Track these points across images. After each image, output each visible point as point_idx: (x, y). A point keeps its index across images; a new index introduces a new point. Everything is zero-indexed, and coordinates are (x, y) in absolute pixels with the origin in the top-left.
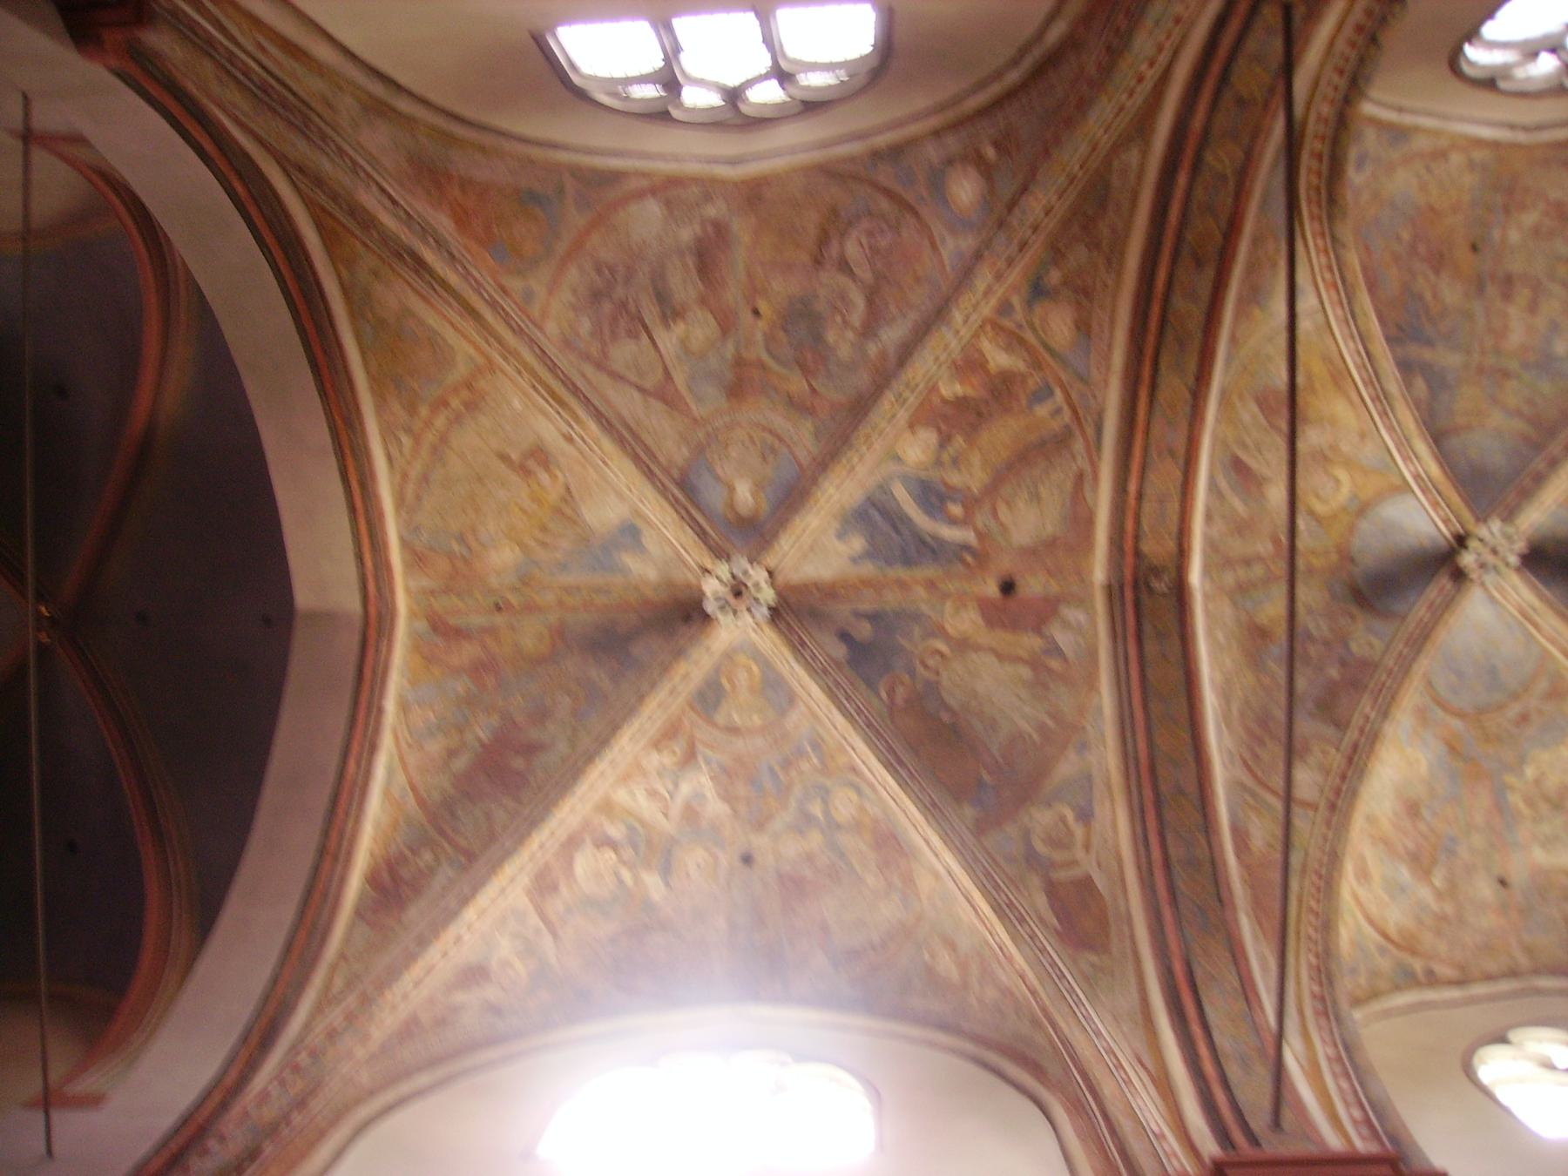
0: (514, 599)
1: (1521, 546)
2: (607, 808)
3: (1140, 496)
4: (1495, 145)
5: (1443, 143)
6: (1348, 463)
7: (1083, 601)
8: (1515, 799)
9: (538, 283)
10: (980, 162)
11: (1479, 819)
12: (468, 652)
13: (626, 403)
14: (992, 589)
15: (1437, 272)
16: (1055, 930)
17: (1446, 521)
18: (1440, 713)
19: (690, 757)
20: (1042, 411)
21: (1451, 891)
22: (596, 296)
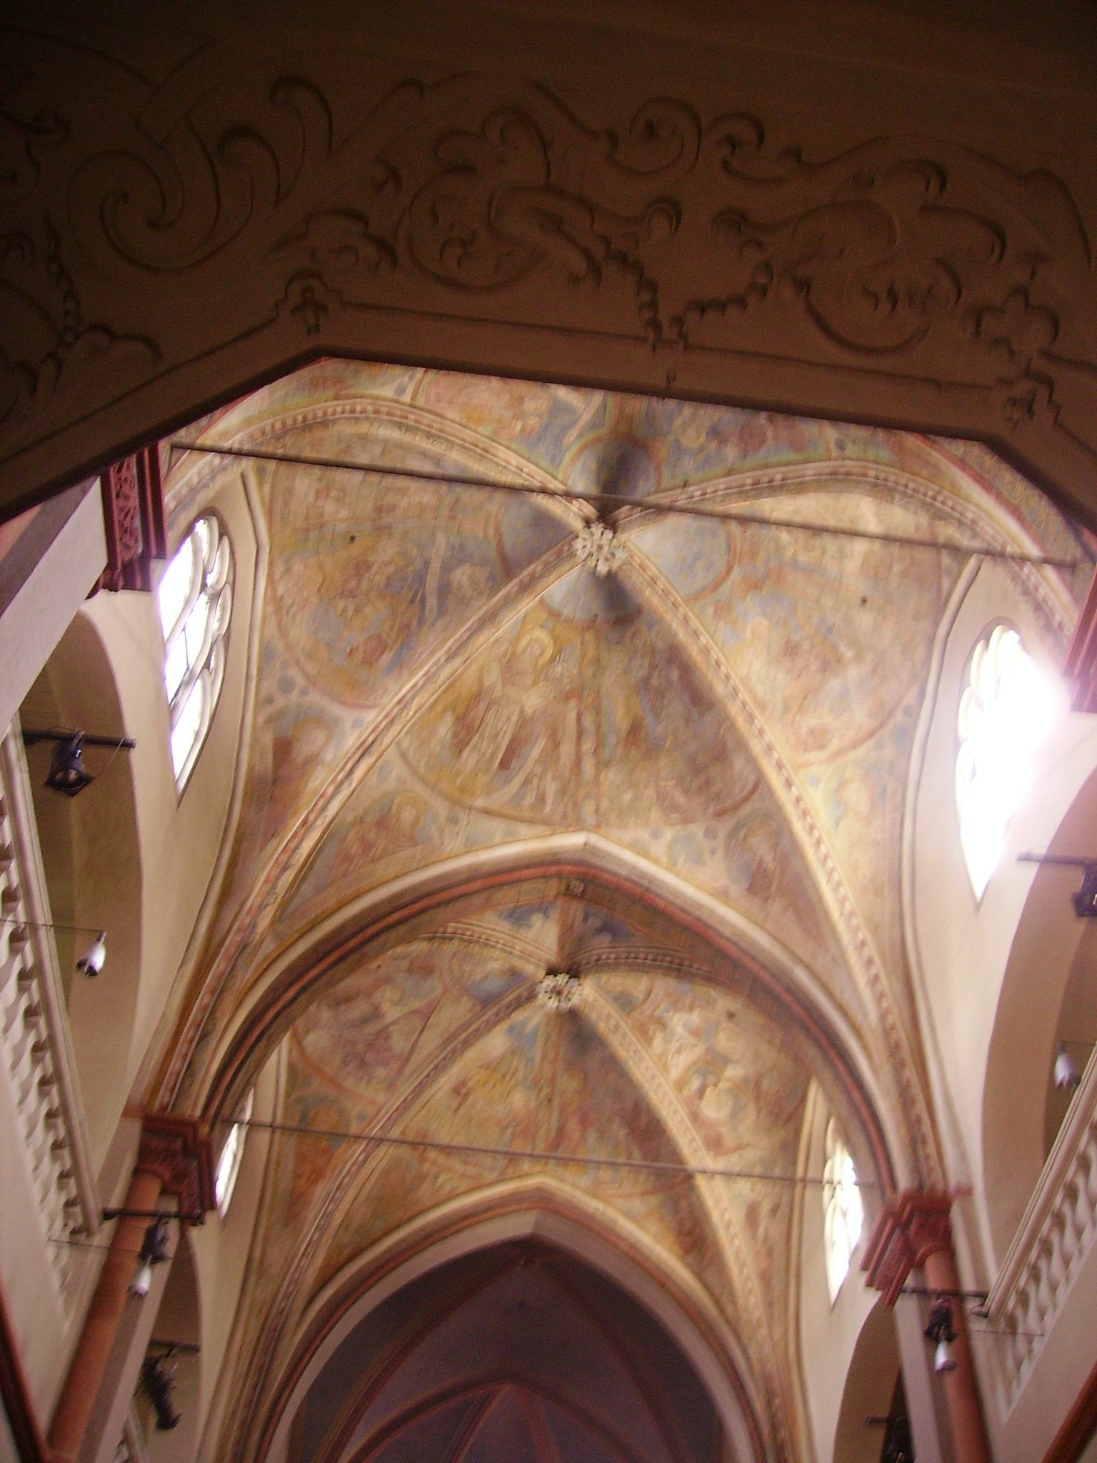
0: (546, 1091)
2: (680, 1085)
5: (271, 609)
9: (355, 1109)
12: (573, 1126)
13: (430, 1041)
18: (726, 587)
19: (662, 1024)
22: (363, 1065)
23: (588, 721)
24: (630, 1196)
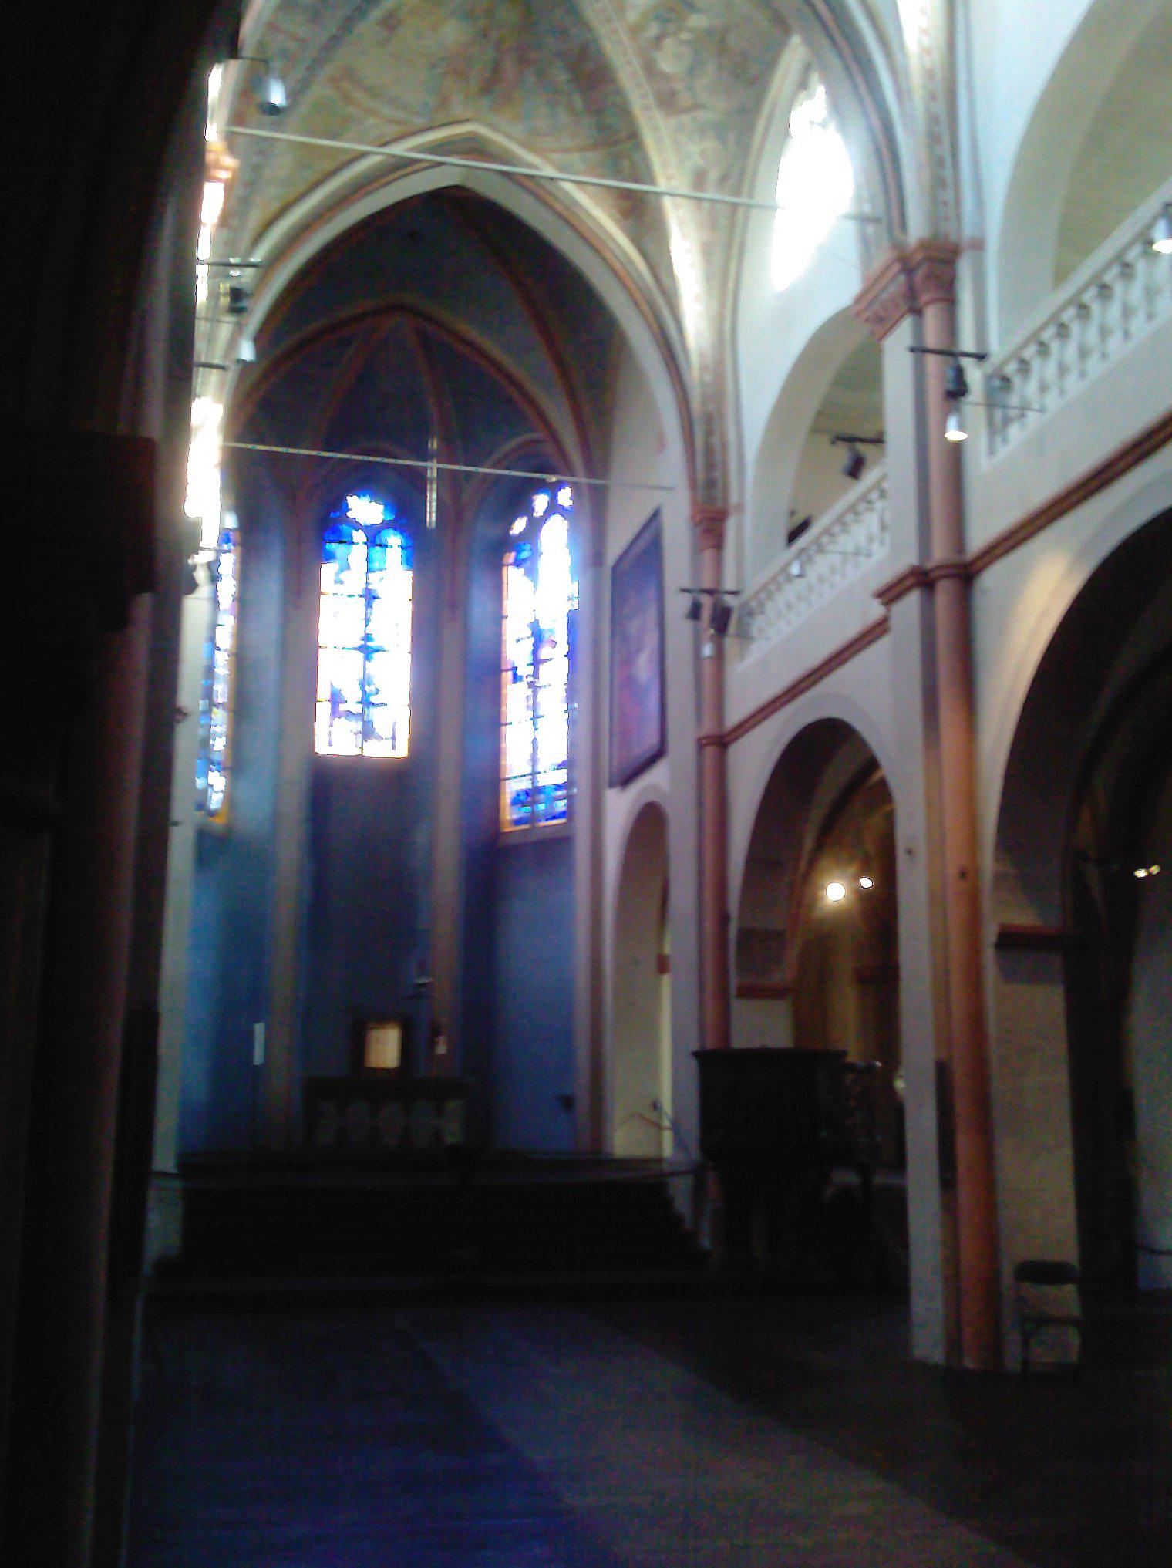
0: (482, 22)
2: (635, 30)
12: (509, 65)
24: (567, 151)
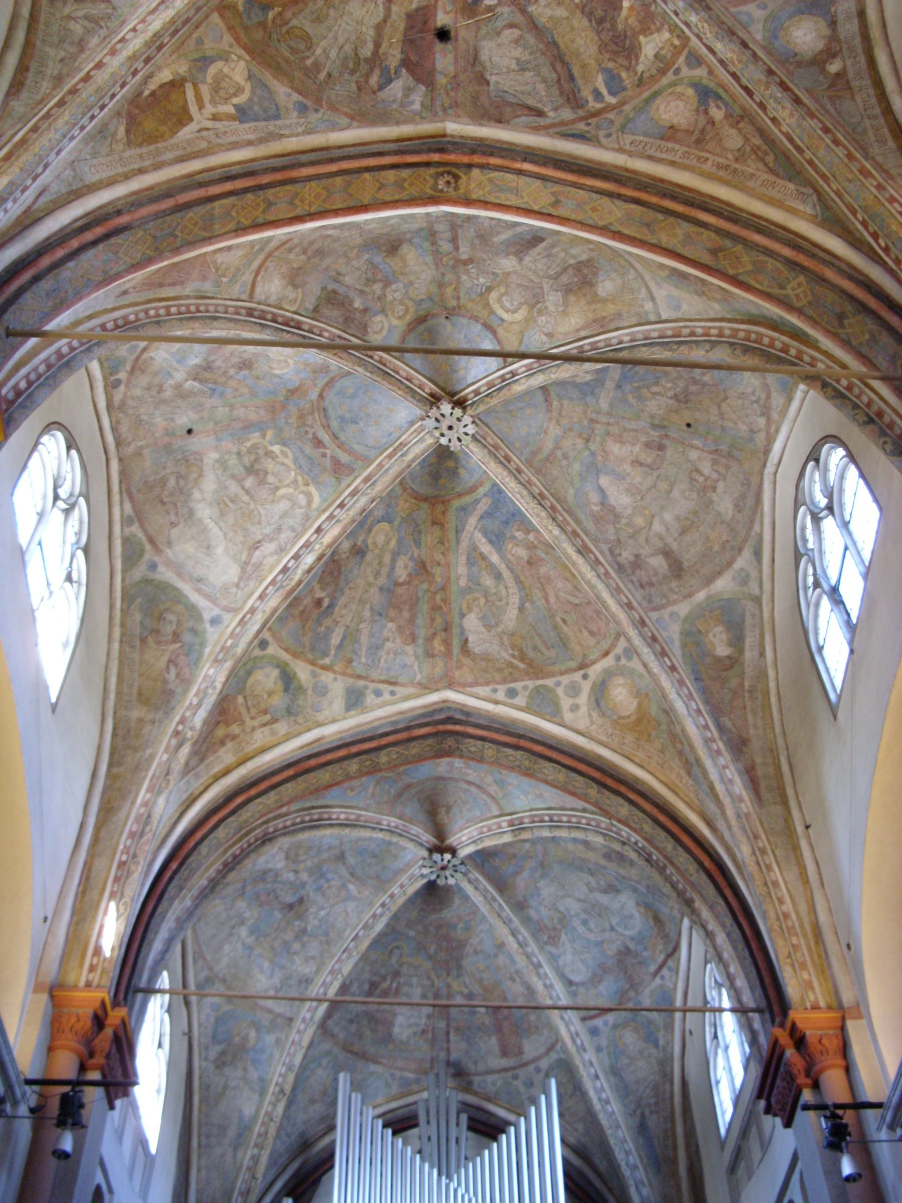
1: (455, 446)
3: (520, 172)
4: (767, 451)
5: (775, 416)
6: (529, 321)
7: (430, 110)
8: (255, 437)
10: (830, 53)
11: (240, 412)
14: (442, 19)
15: (675, 397)
16: (141, 93)
17: (477, 392)
18: (321, 382)
20: (600, 83)
21: (181, 393)
23: (446, 247)
